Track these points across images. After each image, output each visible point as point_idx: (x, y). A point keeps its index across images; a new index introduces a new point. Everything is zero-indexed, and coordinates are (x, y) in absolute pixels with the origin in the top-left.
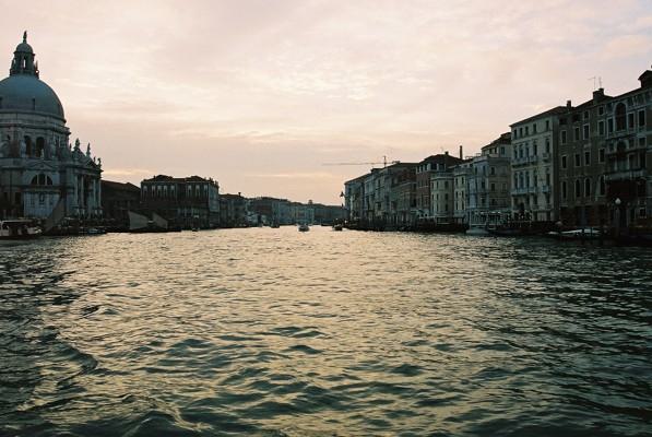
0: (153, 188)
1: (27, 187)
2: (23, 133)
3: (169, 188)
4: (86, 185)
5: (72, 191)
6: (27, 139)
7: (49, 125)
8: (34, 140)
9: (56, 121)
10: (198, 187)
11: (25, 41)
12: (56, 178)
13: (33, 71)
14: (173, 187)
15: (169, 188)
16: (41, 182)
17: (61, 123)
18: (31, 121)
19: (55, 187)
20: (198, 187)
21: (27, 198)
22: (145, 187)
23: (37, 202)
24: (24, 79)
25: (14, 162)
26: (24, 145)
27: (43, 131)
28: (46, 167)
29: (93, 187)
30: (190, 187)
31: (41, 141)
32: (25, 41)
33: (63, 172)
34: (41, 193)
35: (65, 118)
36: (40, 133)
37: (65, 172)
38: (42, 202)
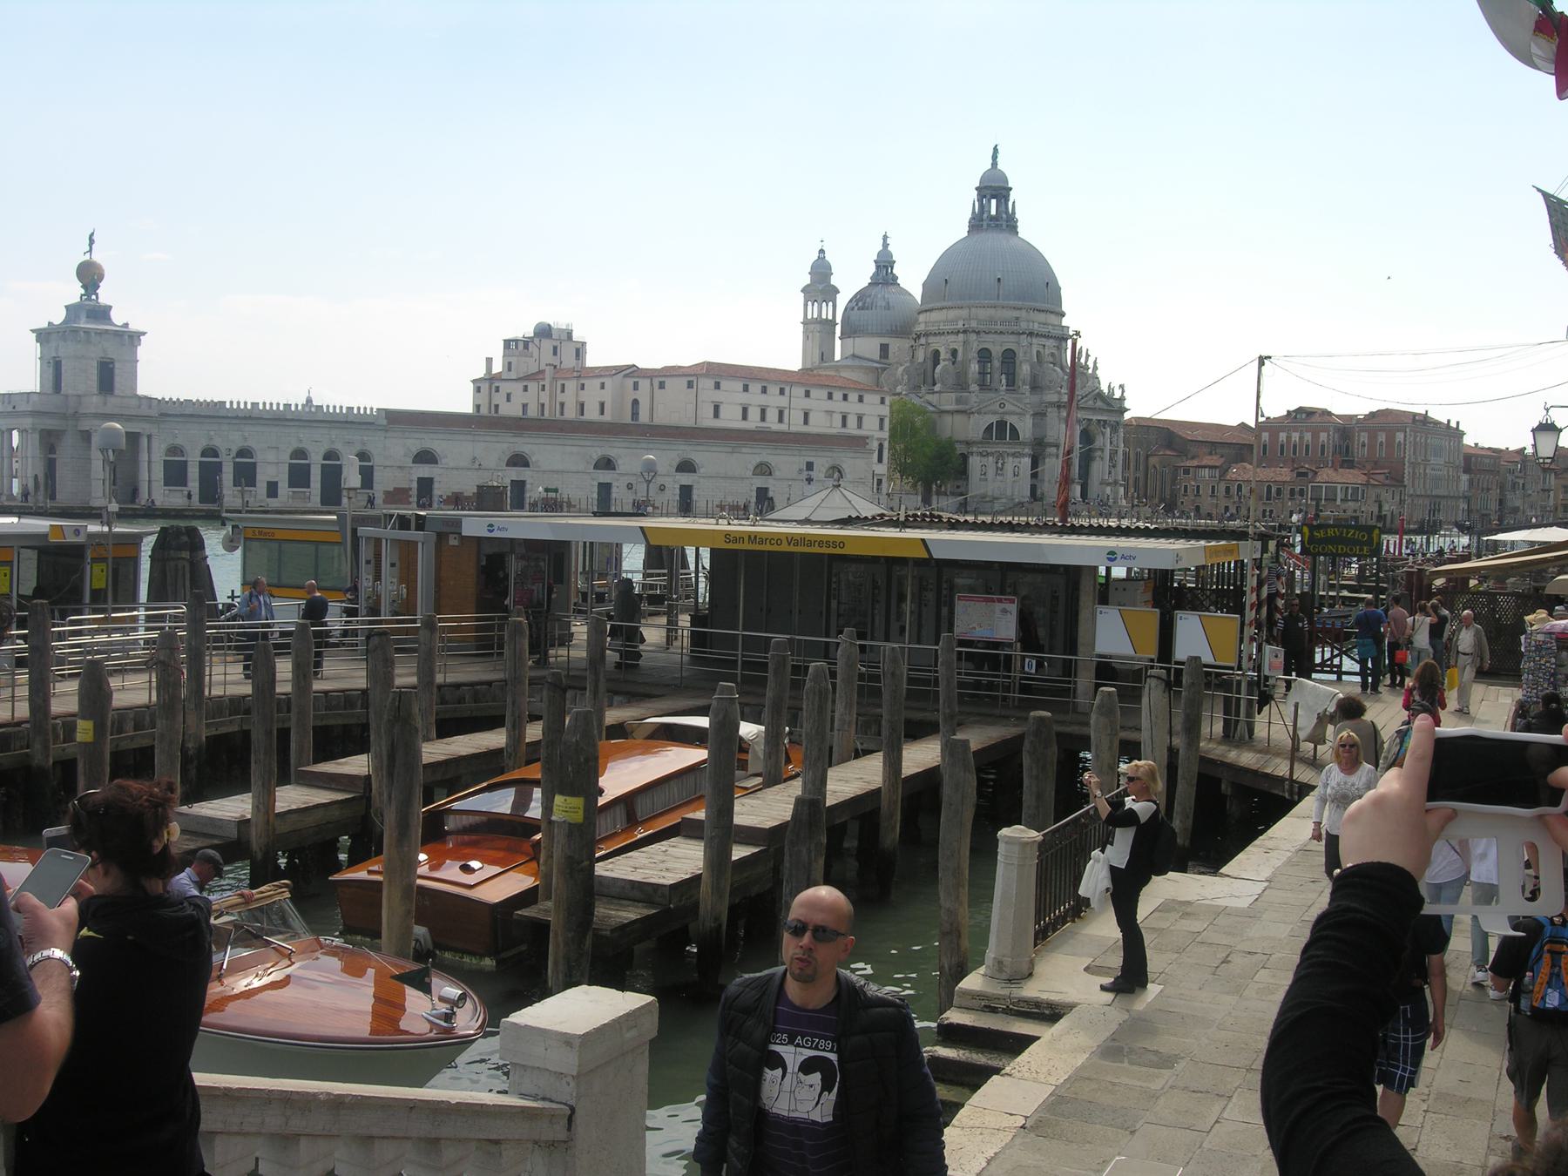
0: (1283, 436)
1: (974, 443)
2: (975, 344)
3: (1315, 436)
4: (1087, 438)
5: (1053, 450)
6: (984, 355)
7: (1024, 325)
8: (997, 351)
9: (1042, 317)
10: (1382, 437)
11: (994, 164)
12: (1025, 427)
13: (1006, 222)
14: (1323, 436)
15: (1315, 436)
16: (1001, 431)
17: (1052, 319)
18: (992, 321)
19: (1023, 444)
20: (1382, 437)
21: (975, 462)
22: (1265, 436)
23: (991, 472)
24: (994, 240)
25: (958, 401)
26: (974, 367)
27: (1012, 338)
28: (1009, 407)
29: (1103, 441)
30: (1364, 437)
31: (1009, 357)
32: (994, 164)
33: (1040, 415)
34: (1001, 455)
35: (1064, 308)
36: (1009, 342)
37: (1044, 415)
38: (1000, 470)
